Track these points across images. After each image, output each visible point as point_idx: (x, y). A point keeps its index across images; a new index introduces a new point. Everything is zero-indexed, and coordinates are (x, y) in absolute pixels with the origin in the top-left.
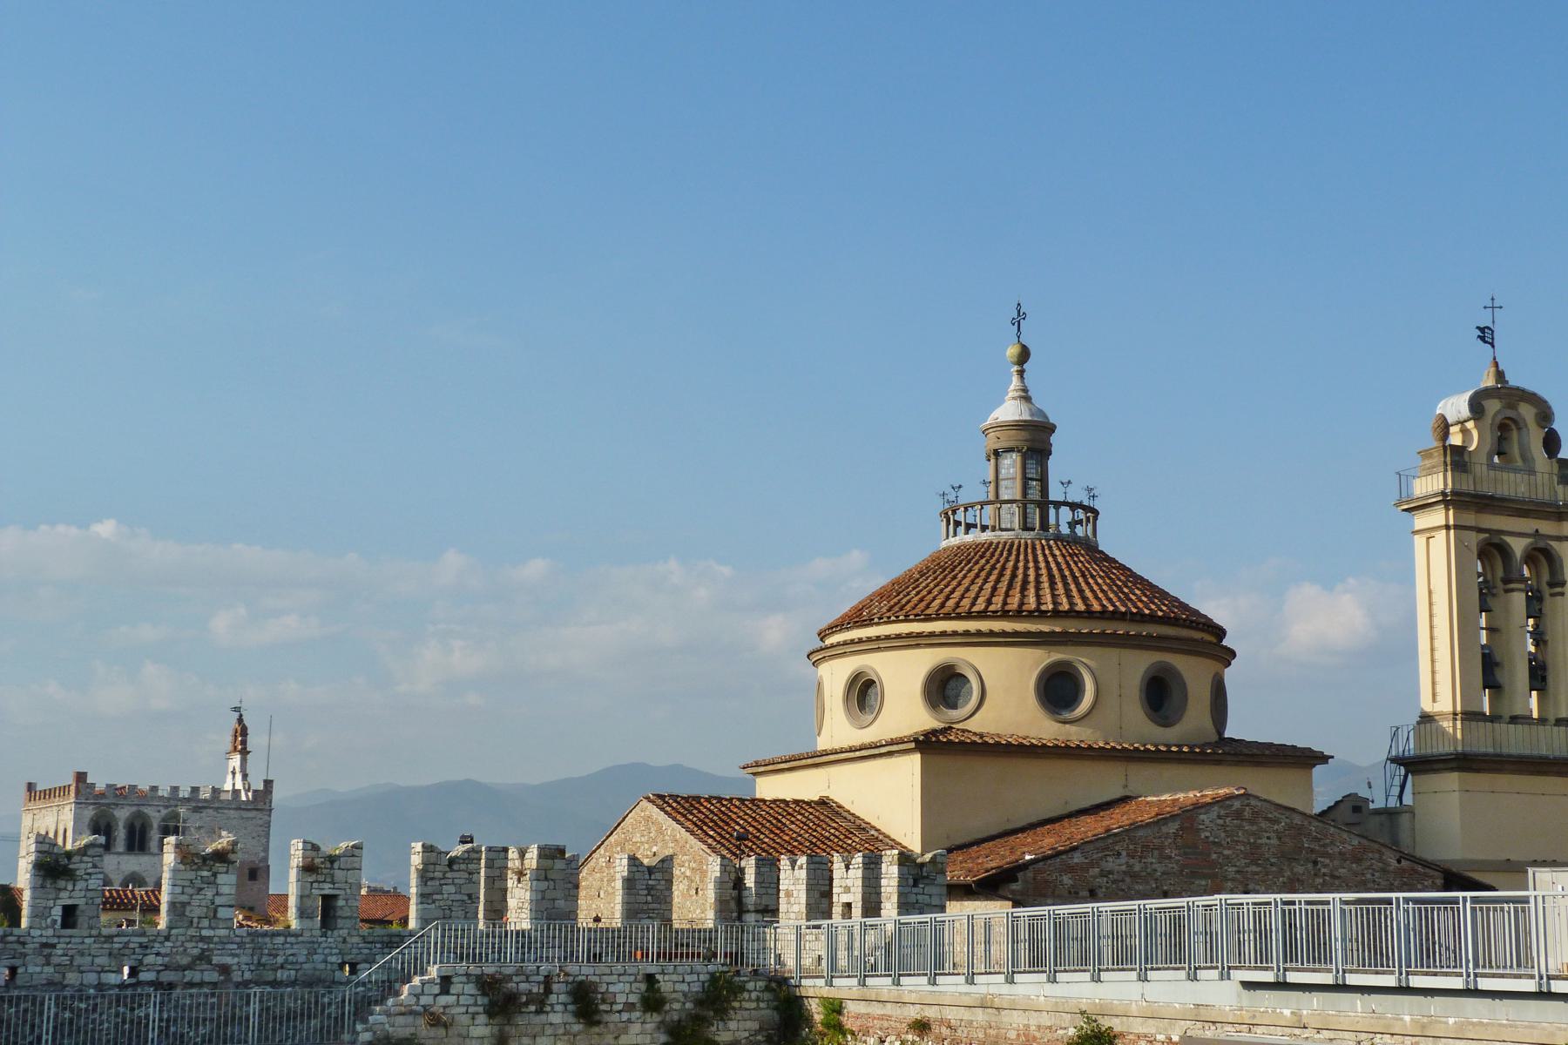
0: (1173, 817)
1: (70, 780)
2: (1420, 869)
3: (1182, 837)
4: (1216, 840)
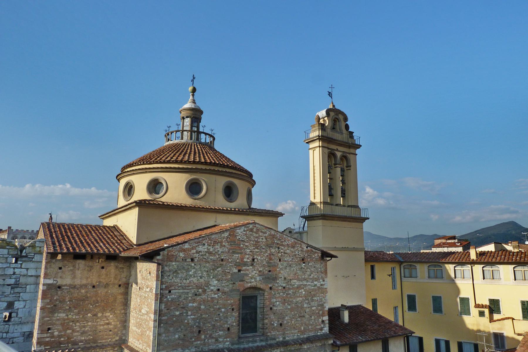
0: (226, 230)
1: (7, 228)
2: (314, 250)
3: (230, 238)
4: (243, 240)
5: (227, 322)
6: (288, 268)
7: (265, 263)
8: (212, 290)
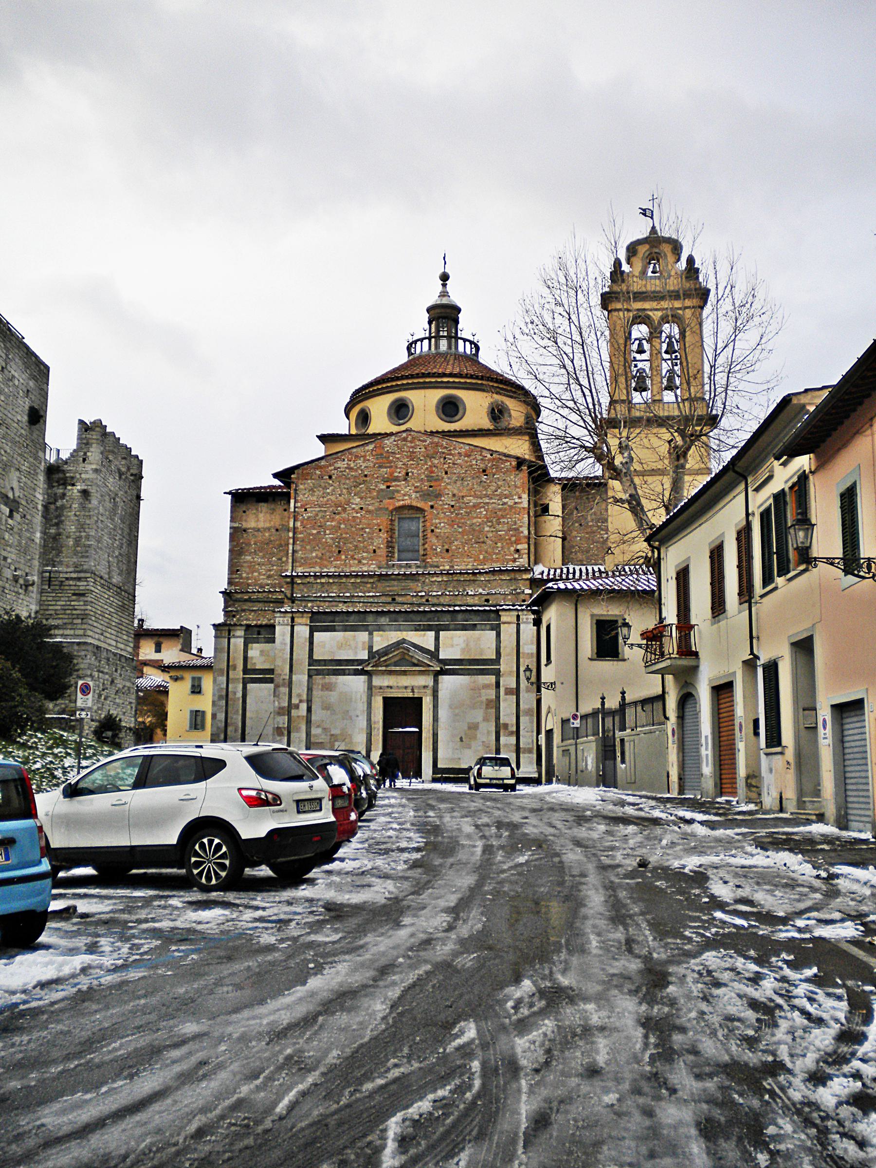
5: (372, 543)
6: (459, 483)
7: (423, 477)
8: (353, 509)
